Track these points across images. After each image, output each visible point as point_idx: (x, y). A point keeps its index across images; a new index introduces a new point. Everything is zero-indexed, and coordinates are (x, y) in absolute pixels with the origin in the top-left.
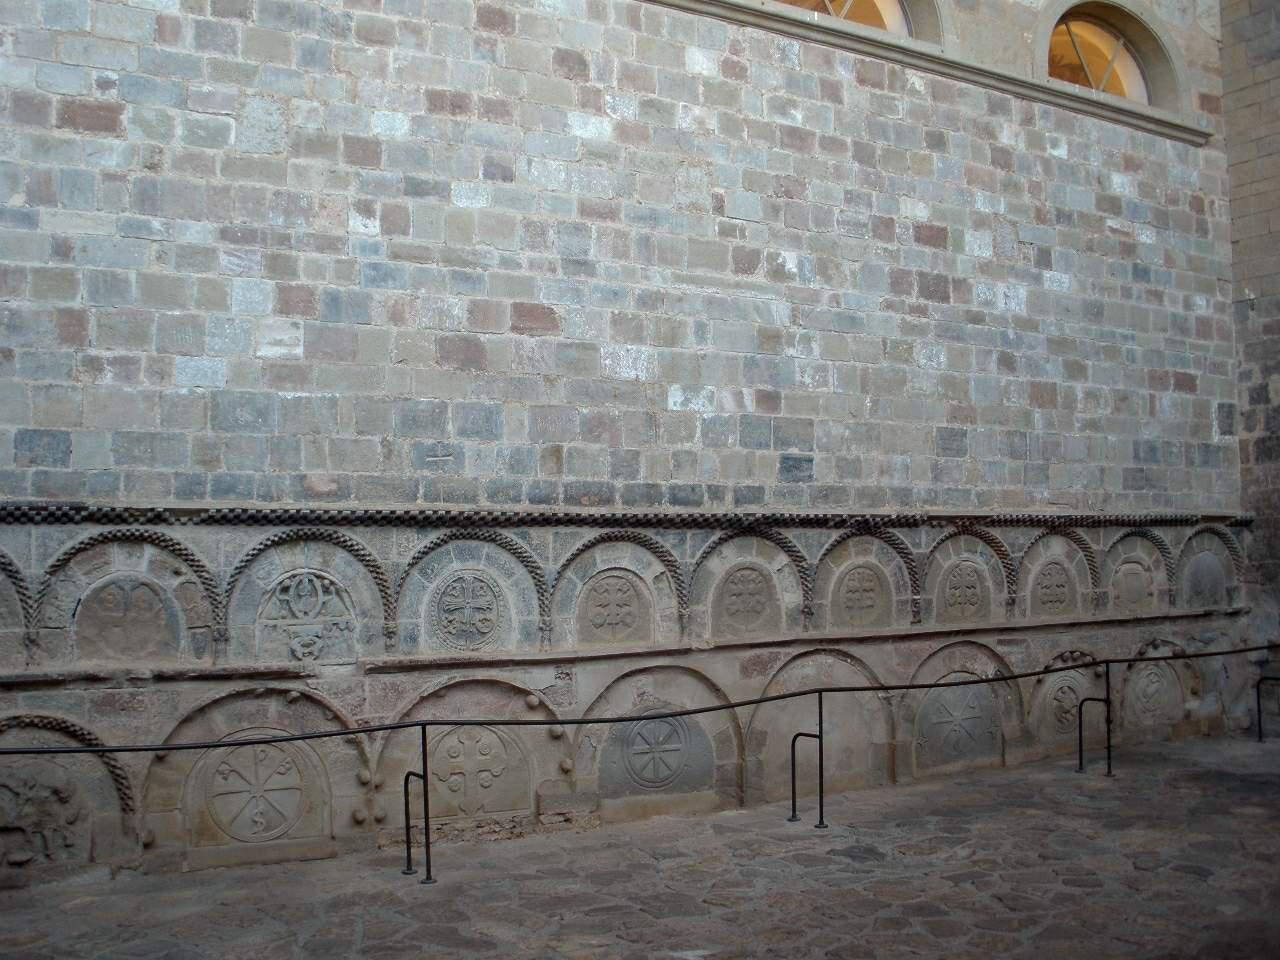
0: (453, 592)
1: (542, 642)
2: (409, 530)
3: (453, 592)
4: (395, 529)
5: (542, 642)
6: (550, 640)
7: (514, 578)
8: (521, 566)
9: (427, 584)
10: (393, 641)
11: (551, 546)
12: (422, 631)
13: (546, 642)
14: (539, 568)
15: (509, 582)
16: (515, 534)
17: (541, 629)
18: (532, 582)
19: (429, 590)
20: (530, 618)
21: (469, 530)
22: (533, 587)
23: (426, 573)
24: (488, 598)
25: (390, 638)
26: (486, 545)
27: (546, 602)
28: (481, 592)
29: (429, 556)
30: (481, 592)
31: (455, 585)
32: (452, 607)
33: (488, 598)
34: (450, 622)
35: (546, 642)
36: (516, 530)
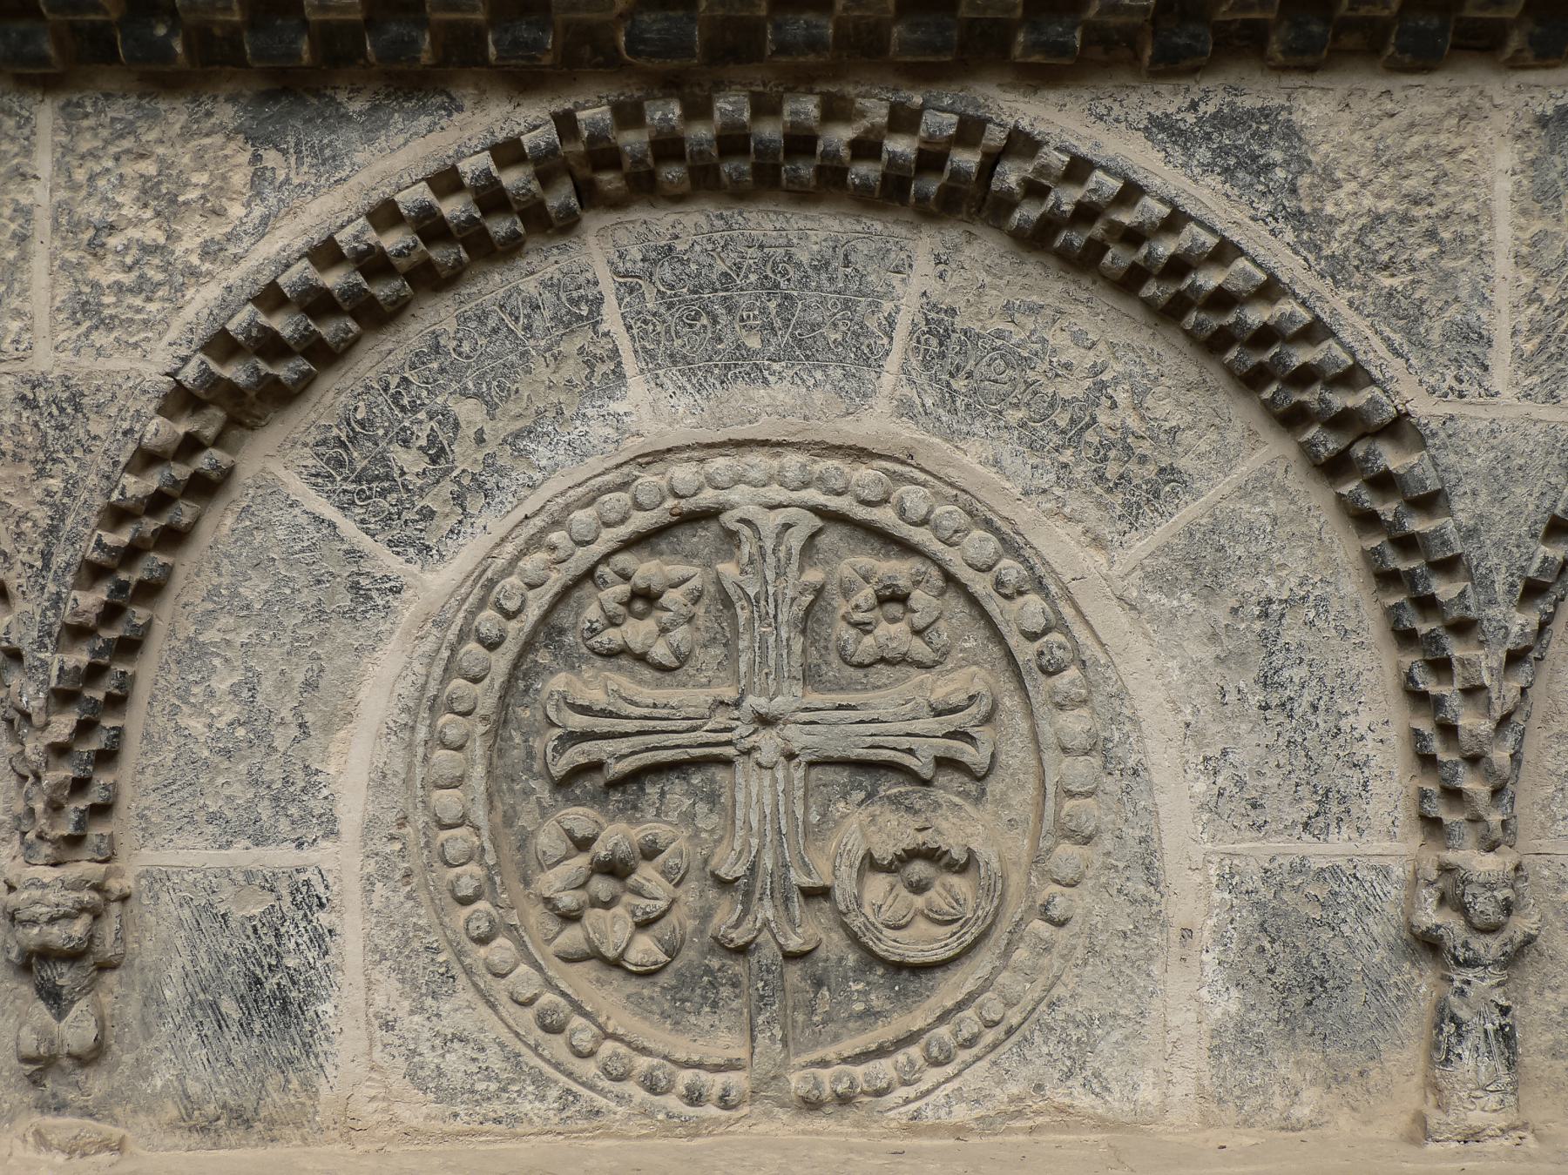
0: (637, 632)
1: (1441, 1054)
2: (177, 115)
3: (637, 632)
4: (45, 115)
5: (1441, 1054)
6: (1506, 1036)
7: (1189, 511)
8: (1241, 414)
9: (389, 562)
10: (77, 1030)
11: (1504, 234)
12: (351, 946)
13: (1472, 1064)
14: (1398, 428)
15: (1140, 546)
16: (1161, 128)
17: (1428, 945)
18: (1346, 547)
19: (408, 610)
20: (1335, 847)
21: (730, 106)
22: (1352, 586)
23: (381, 478)
24: (946, 686)
25: (53, 997)
26: (925, 244)
27: (1472, 722)
28: (892, 633)
29: (412, 334)
30: (892, 633)
31: (647, 569)
32: (619, 757)
33: (946, 686)
34: (616, 869)
35: (1472, 1064)
36: (1168, 101)
